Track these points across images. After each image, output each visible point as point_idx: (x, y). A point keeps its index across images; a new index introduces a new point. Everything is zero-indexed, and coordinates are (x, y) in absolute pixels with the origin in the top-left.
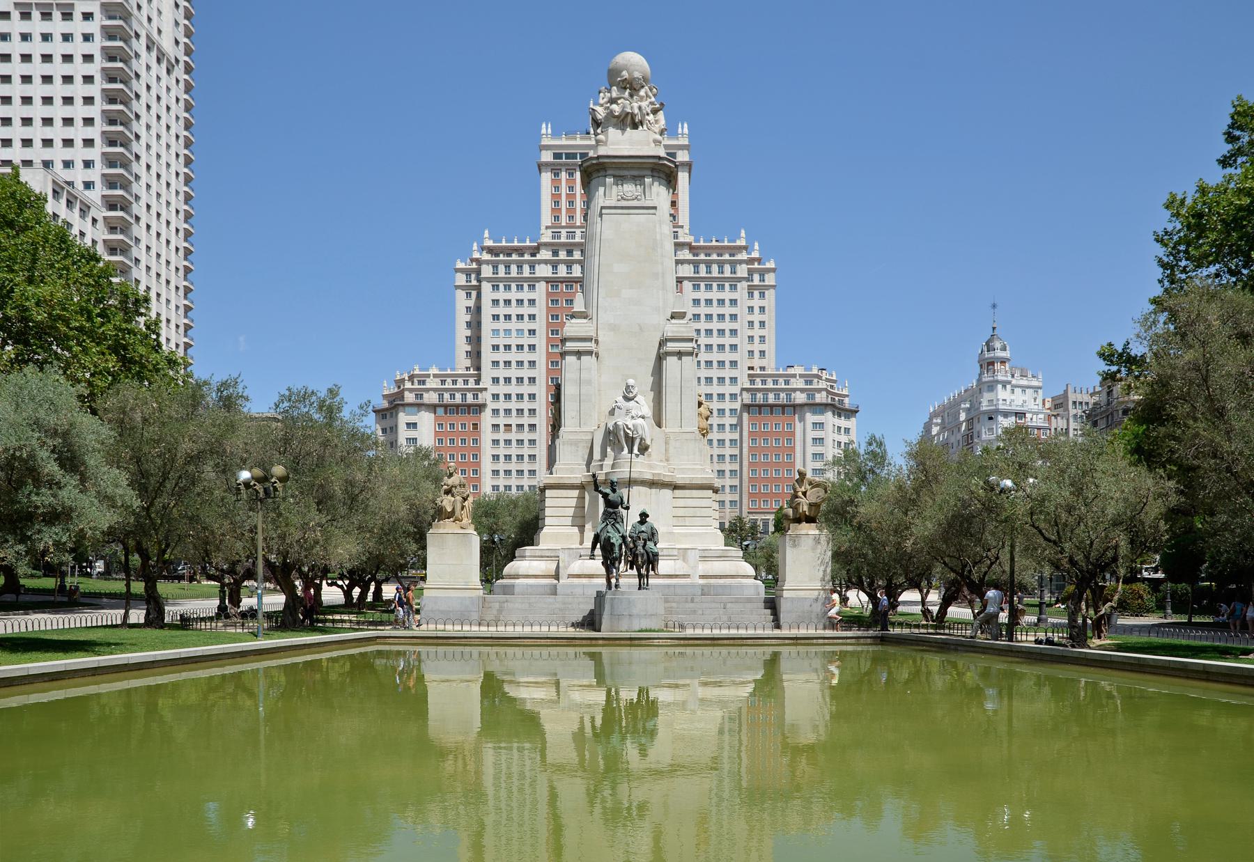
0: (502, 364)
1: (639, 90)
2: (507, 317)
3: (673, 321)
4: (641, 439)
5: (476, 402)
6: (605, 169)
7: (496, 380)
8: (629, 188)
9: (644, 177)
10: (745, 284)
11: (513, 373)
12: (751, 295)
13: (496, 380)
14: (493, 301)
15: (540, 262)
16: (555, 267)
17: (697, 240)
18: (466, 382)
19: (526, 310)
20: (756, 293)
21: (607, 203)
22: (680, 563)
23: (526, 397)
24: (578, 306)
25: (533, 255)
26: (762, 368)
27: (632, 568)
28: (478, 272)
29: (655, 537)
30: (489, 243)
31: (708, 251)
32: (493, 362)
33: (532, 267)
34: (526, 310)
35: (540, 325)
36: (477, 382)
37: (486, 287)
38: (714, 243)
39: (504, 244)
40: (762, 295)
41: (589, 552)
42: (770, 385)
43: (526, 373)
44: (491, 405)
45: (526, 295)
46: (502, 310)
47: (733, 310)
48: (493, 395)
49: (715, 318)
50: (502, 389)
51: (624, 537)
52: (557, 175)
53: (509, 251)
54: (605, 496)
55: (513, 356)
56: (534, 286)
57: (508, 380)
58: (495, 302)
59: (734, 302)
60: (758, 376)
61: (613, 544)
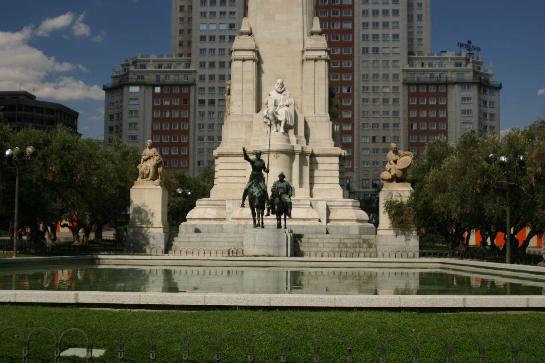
2: (213, 14)
3: (312, 37)
4: (286, 121)
5: (186, 81)
7: (202, 65)
24: (244, 28)
27: (273, 213)
29: (290, 192)
36: (188, 66)
42: (427, 67)
44: (199, 85)
49: (380, 13)
50: (207, 72)
54: (252, 162)
57: (212, 65)
61: (255, 196)
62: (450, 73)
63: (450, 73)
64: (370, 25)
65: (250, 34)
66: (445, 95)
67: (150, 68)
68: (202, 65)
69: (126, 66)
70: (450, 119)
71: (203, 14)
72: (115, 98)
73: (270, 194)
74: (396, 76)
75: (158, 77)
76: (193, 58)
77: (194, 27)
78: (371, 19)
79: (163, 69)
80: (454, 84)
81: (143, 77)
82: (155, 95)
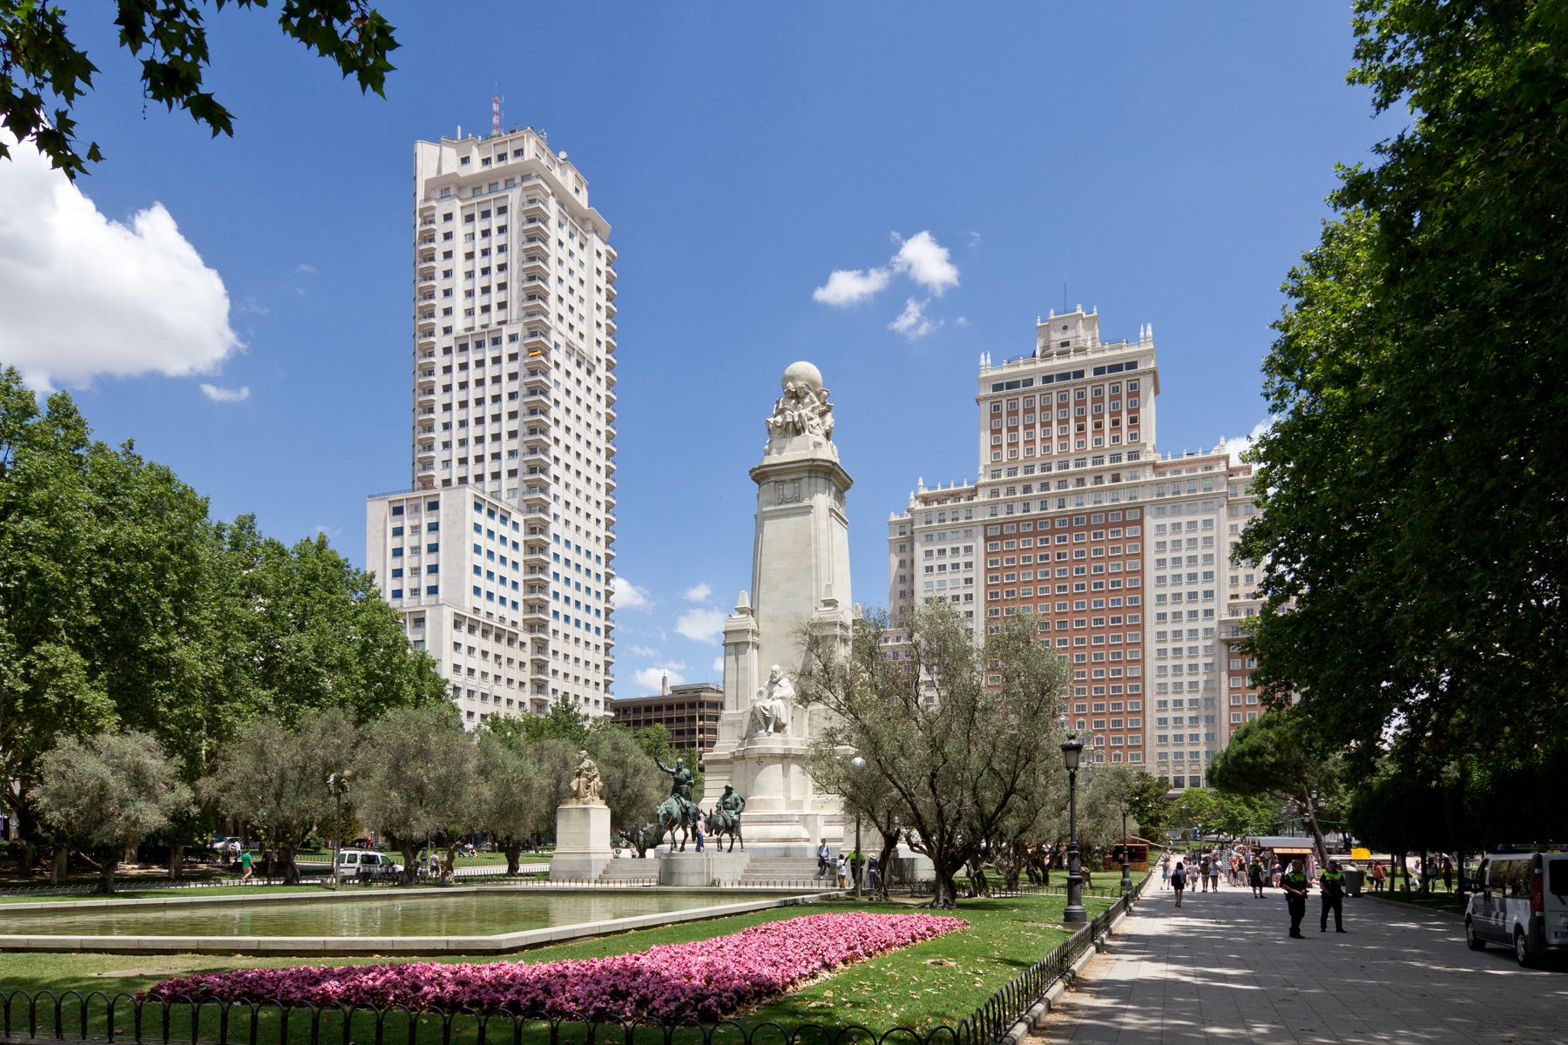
6: (767, 477)
8: (788, 490)
15: (977, 505)
16: (993, 506)
17: (1165, 457)
25: (970, 498)
30: (924, 491)
31: (1177, 468)
35: (978, 573)
38: (1185, 458)
39: (939, 490)
46: (935, 562)
53: (941, 499)
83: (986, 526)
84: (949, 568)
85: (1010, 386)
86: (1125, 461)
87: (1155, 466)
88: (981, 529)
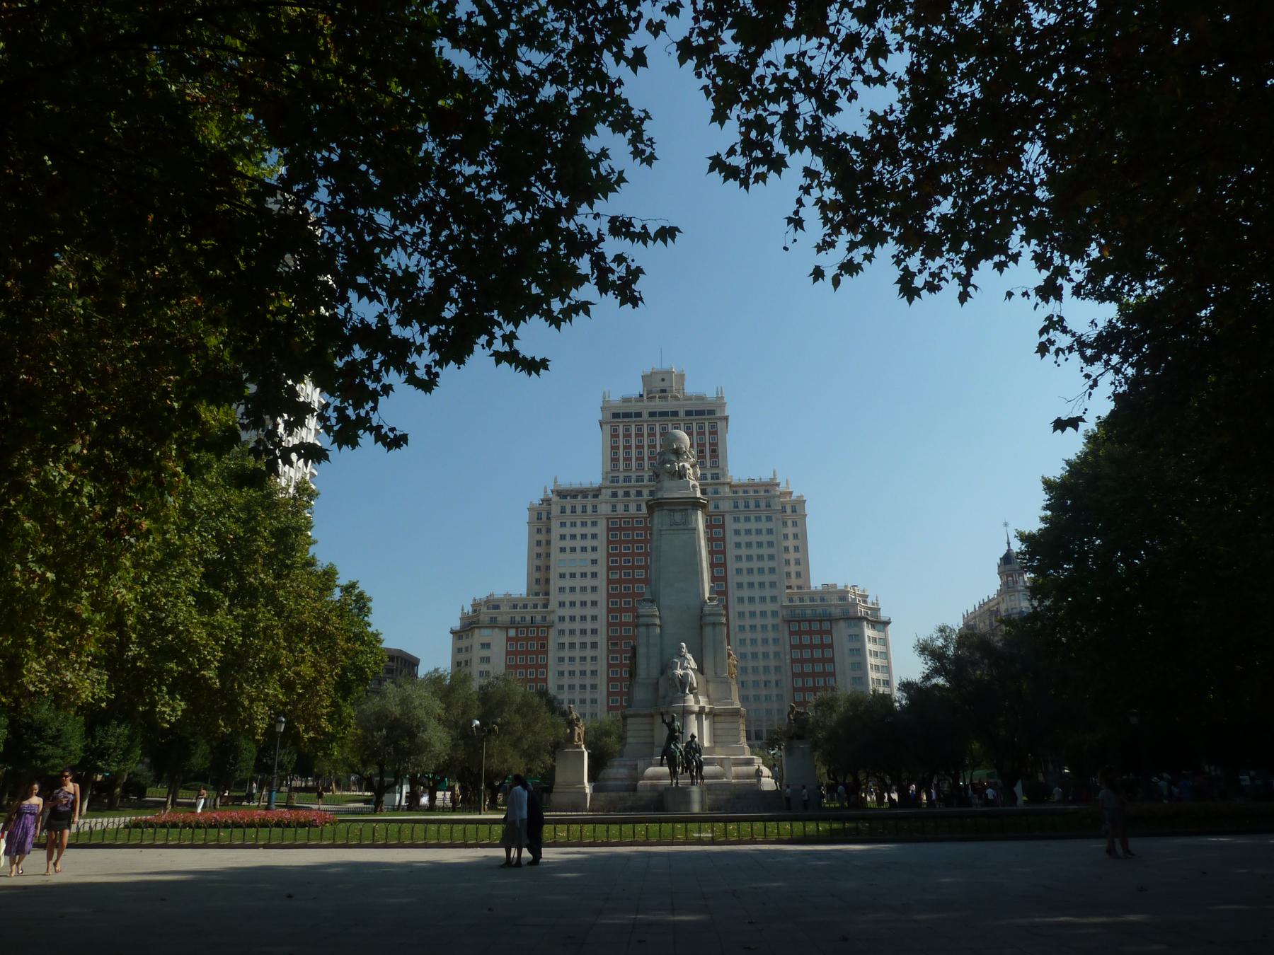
0: (567, 590)
1: (682, 455)
2: (573, 550)
8: (678, 517)
9: (687, 510)
10: (780, 515)
11: (578, 597)
12: (785, 524)
13: (562, 604)
14: (561, 536)
18: (535, 606)
19: (589, 543)
20: (790, 523)
21: (665, 528)
22: (718, 767)
23: (589, 619)
25: (596, 496)
26: (799, 587)
28: (549, 513)
32: (560, 588)
33: (595, 509)
34: (589, 543)
35: (601, 555)
36: (545, 606)
37: (555, 525)
40: (795, 524)
41: (659, 762)
43: (589, 597)
45: (589, 530)
46: (568, 543)
47: (770, 538)
48: (560, 617)
51: (681, 752)
52: (615, 430)
55: (578, 582)
56: (596, 522)
58: (563, 537)
59: (770, 531)
60: (796, 594)
62: (833, 608)
63: (833, 608)
64: (744, 558)
65: (652, 601)
66: (830, 632)
67: (504, 609)
68: (562, 604)
69: (476, 606)
70: (836, 660)
71: (563, 550)
72: (464, 643)
73: (684, 753)
74: (774, 614)
75: (513, 619)
76: (551, 597)
77: (552, 564)
78: (743, 552)
79: (518, 610)
80: (837, 620)
81: (496, 618)
82: (509, 639)
83: (608, 519)
84: (578, 550)
85: (627, 415)
86: (709, 481)
87: (729, 484)
88: (605, 522)
